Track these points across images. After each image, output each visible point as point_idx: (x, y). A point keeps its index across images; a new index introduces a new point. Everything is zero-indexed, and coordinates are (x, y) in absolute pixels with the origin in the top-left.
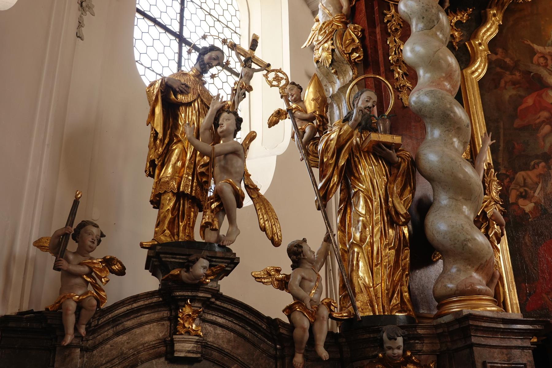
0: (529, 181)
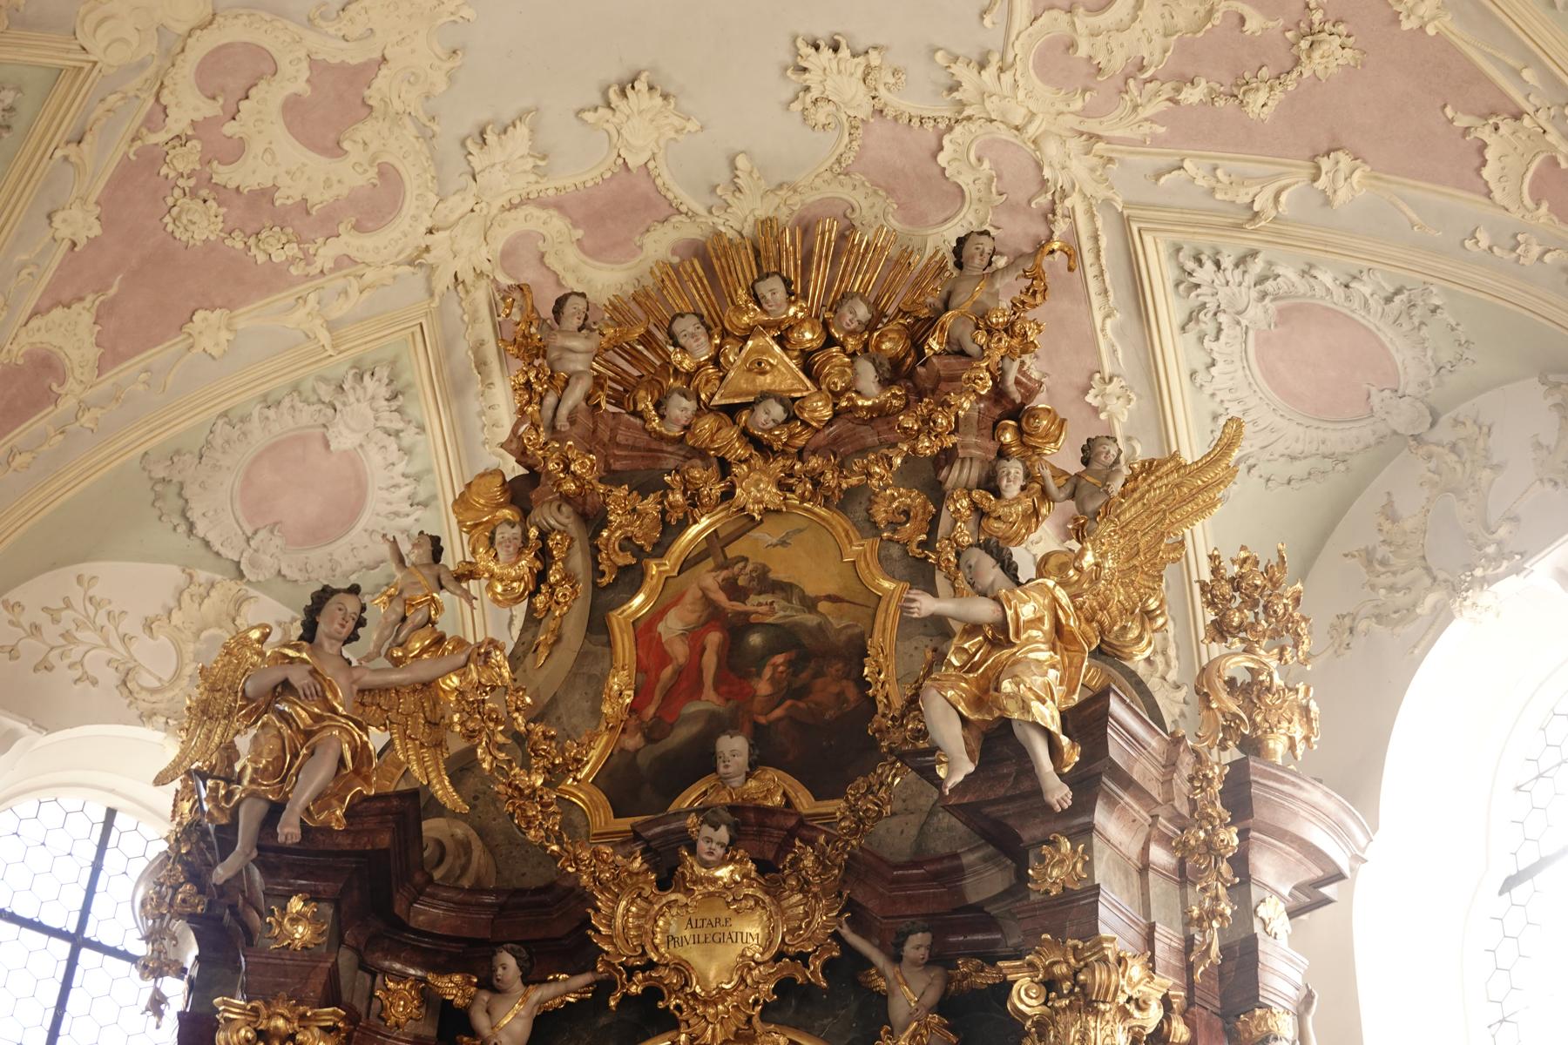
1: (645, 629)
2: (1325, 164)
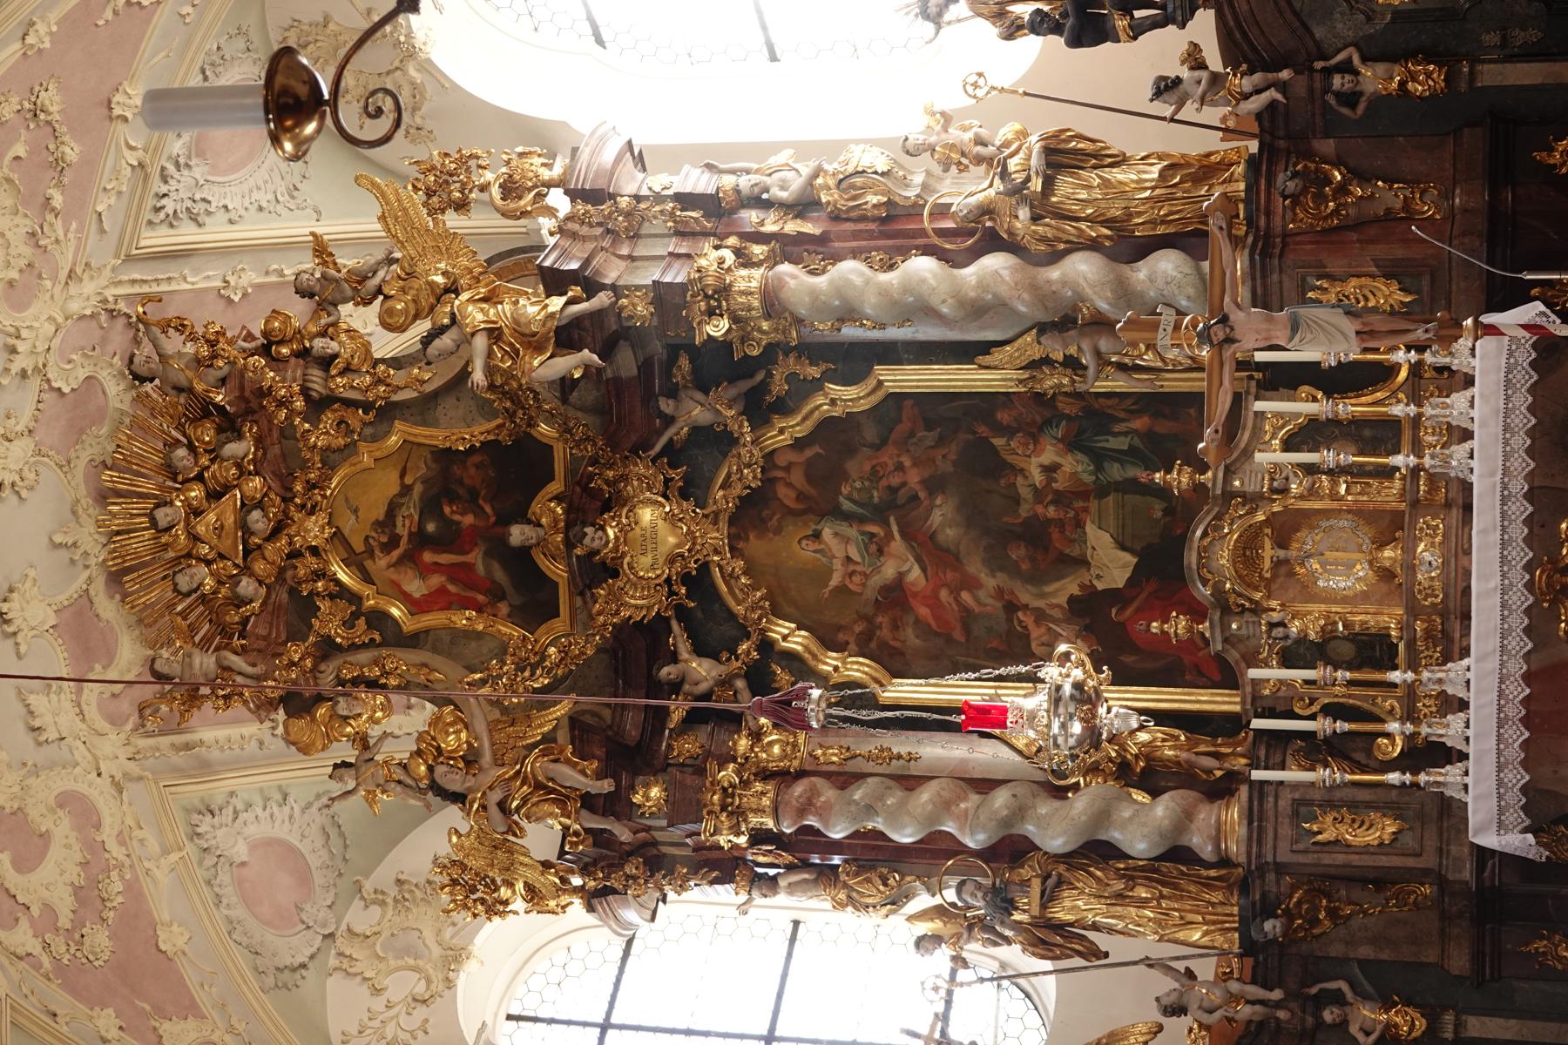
0: (1045, 639)
1: (416, 606)
2: (117, 111)
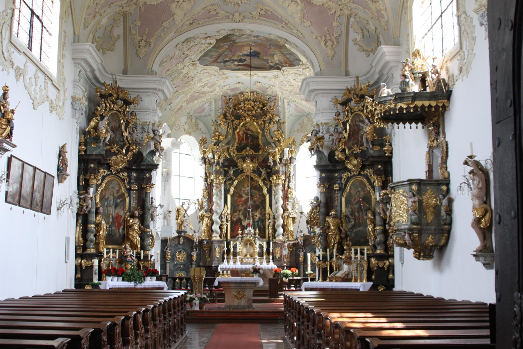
1: (238, 133)
